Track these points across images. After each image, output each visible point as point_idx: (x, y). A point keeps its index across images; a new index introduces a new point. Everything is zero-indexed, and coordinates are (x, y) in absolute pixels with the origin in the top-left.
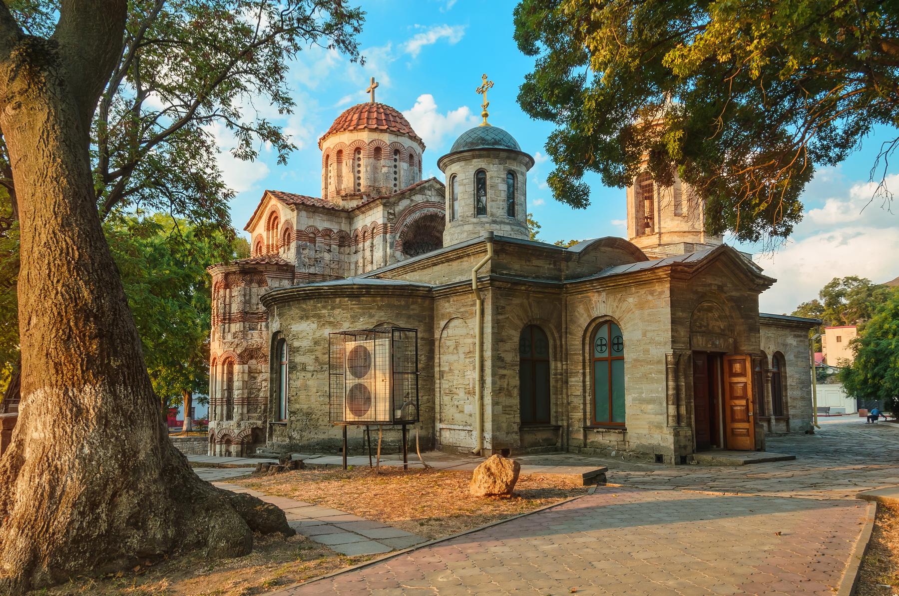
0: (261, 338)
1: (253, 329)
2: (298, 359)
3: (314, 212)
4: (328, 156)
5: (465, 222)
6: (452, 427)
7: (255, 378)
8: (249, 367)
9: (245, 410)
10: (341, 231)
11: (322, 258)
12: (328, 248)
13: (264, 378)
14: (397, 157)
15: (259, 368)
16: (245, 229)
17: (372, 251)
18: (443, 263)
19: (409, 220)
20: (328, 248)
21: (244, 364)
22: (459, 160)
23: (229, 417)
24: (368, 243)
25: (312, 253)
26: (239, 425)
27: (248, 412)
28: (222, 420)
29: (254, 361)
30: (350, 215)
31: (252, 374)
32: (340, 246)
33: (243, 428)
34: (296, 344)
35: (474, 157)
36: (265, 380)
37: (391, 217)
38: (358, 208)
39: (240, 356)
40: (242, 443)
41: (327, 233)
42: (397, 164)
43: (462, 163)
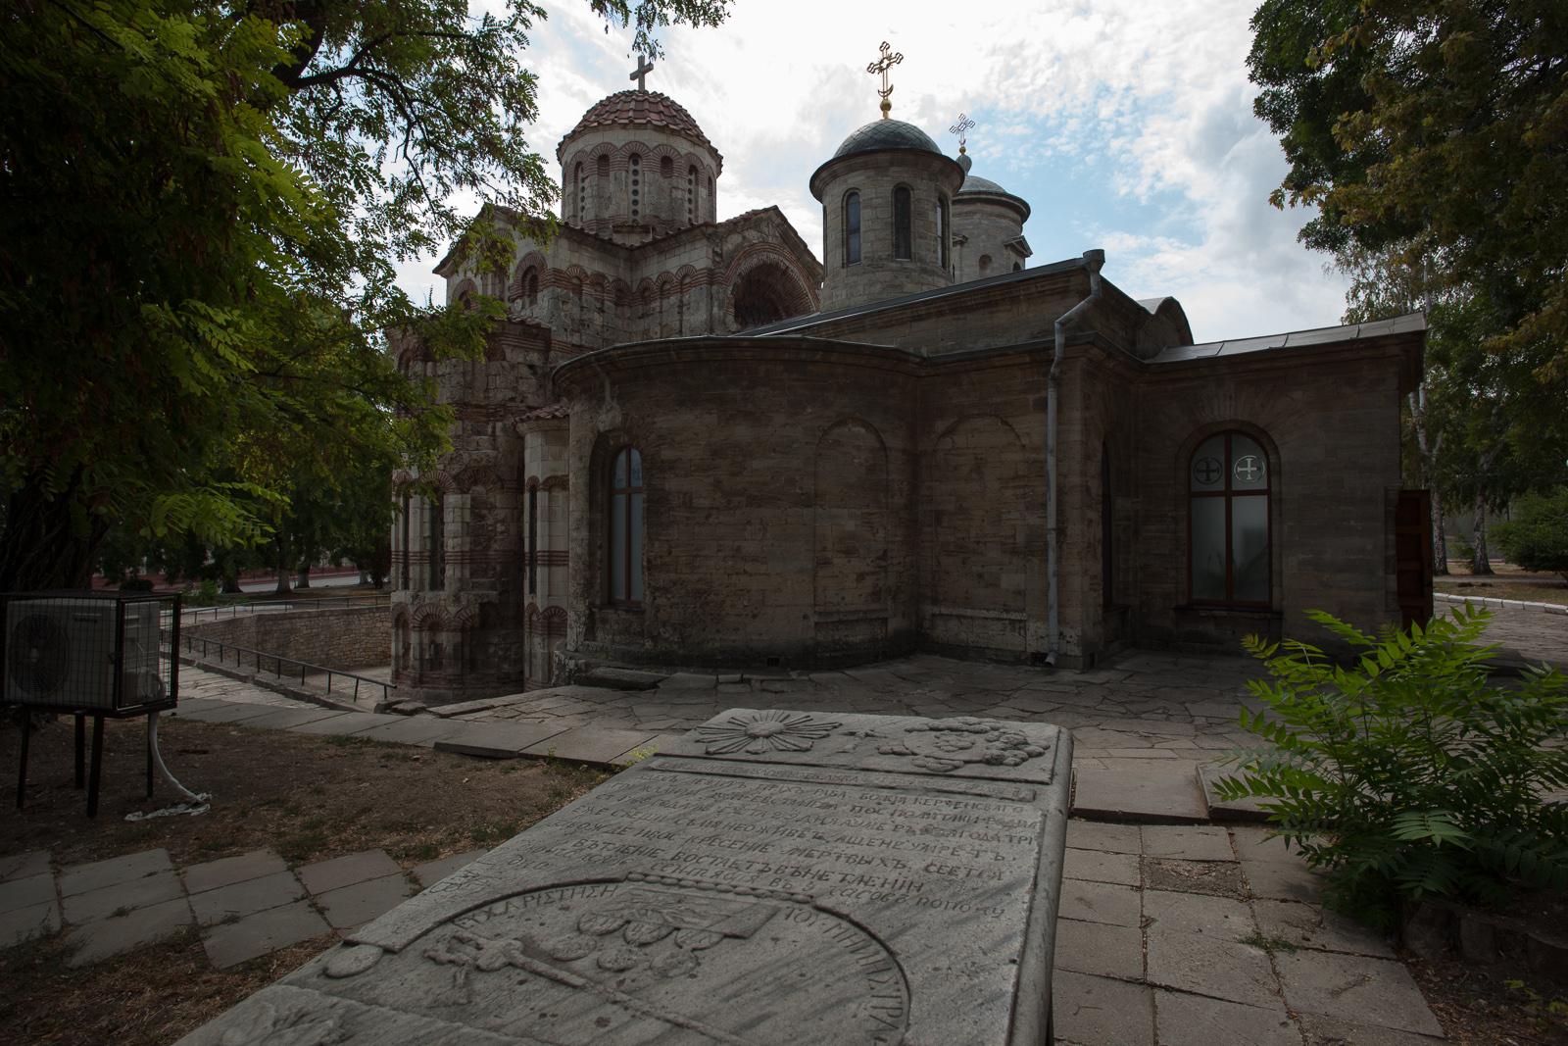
0: (495, 448)
1: (479, 433)
2: (672, 484)
3: (580, 243)
4: (579, 164)
5: (876, 265)
6: (969, 612)
7: (483, 517)
8: (473, 499)
9: (467, 573)
10: (618, 280)
11: (591, 320)
12: (598, 305)
13: (500, 517)
14: (693, 177)
15: (492, 499)
16: (436, 271)
17: (680, 313)
18: (940, 314)
19: (746, 265)
20: (598, 305)
21: (463, 492)
22: (865, 167)
23: (437, 584)
24: (673, 299)
25: (576, 311)
26: (457, 599)
27: (472, 575)
28: (422, 589)
29: (479, 489)
30: (633, 257)
31: (478, 509)
32: (617, 304)
33: (464, 603)
34: (667, 454)
35: (892, 164)
36: (503, 521)
37: (717, 259)
38: (644, 246)
39: (455, 478)
40: (463, 630)
41: (598, 280)
42: (692, 187)
43: (872, 173)
